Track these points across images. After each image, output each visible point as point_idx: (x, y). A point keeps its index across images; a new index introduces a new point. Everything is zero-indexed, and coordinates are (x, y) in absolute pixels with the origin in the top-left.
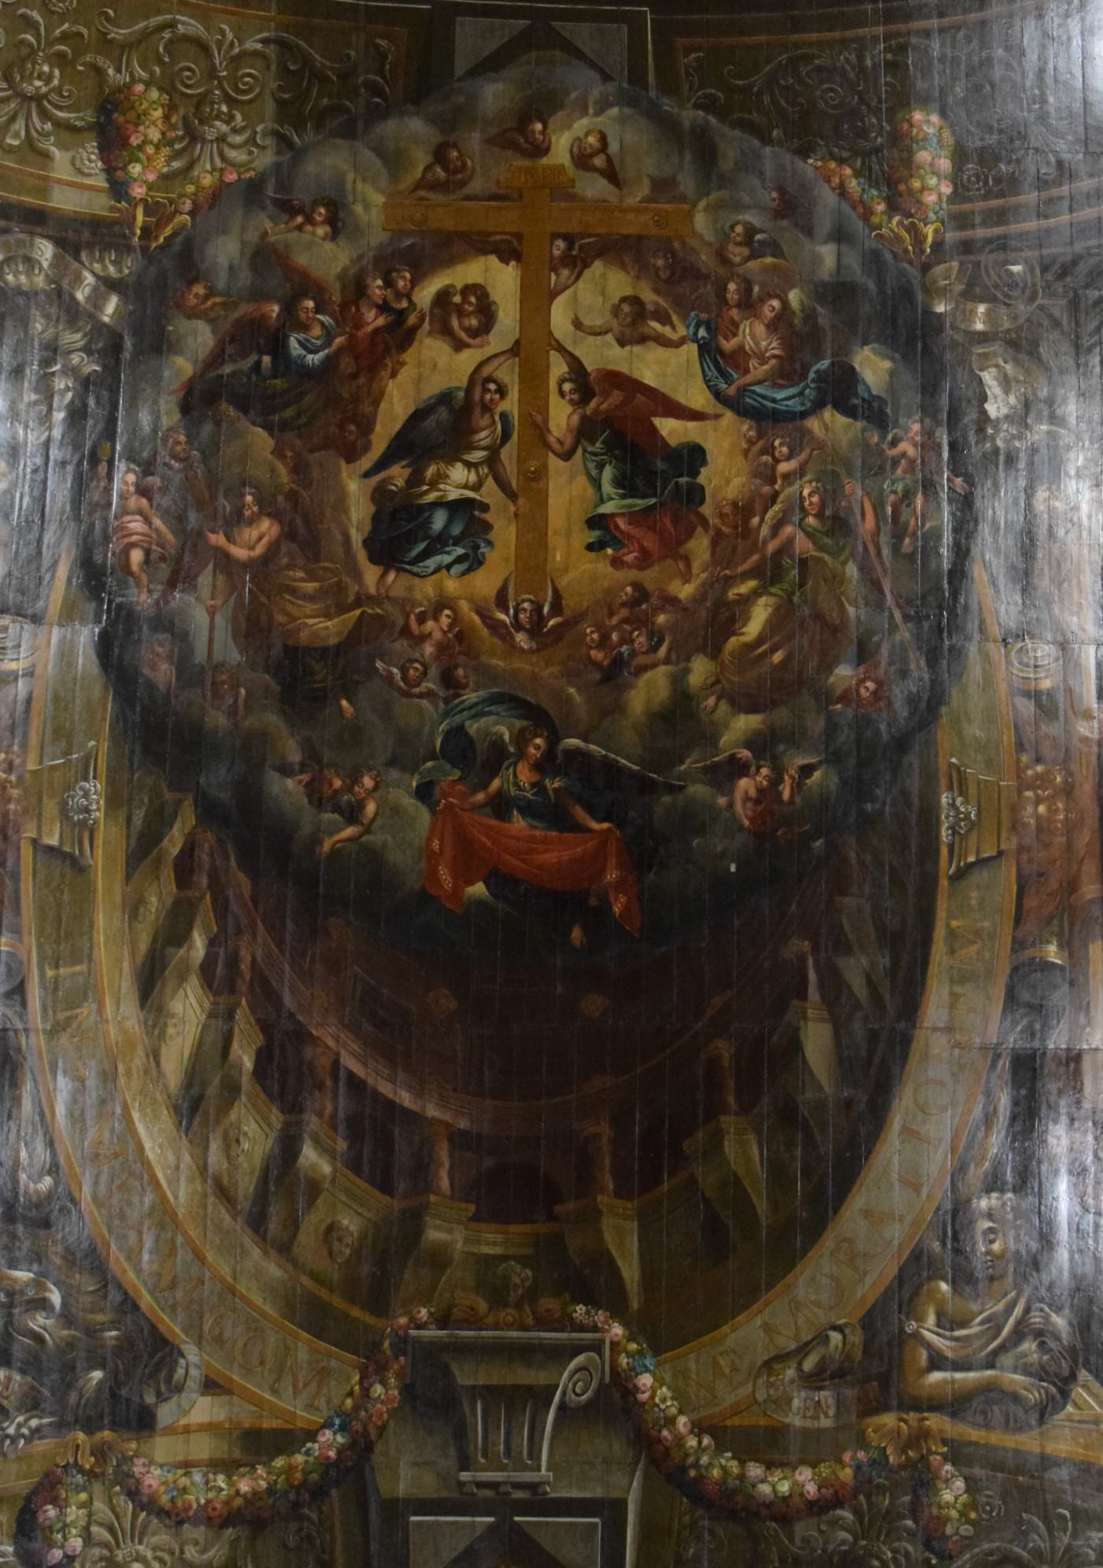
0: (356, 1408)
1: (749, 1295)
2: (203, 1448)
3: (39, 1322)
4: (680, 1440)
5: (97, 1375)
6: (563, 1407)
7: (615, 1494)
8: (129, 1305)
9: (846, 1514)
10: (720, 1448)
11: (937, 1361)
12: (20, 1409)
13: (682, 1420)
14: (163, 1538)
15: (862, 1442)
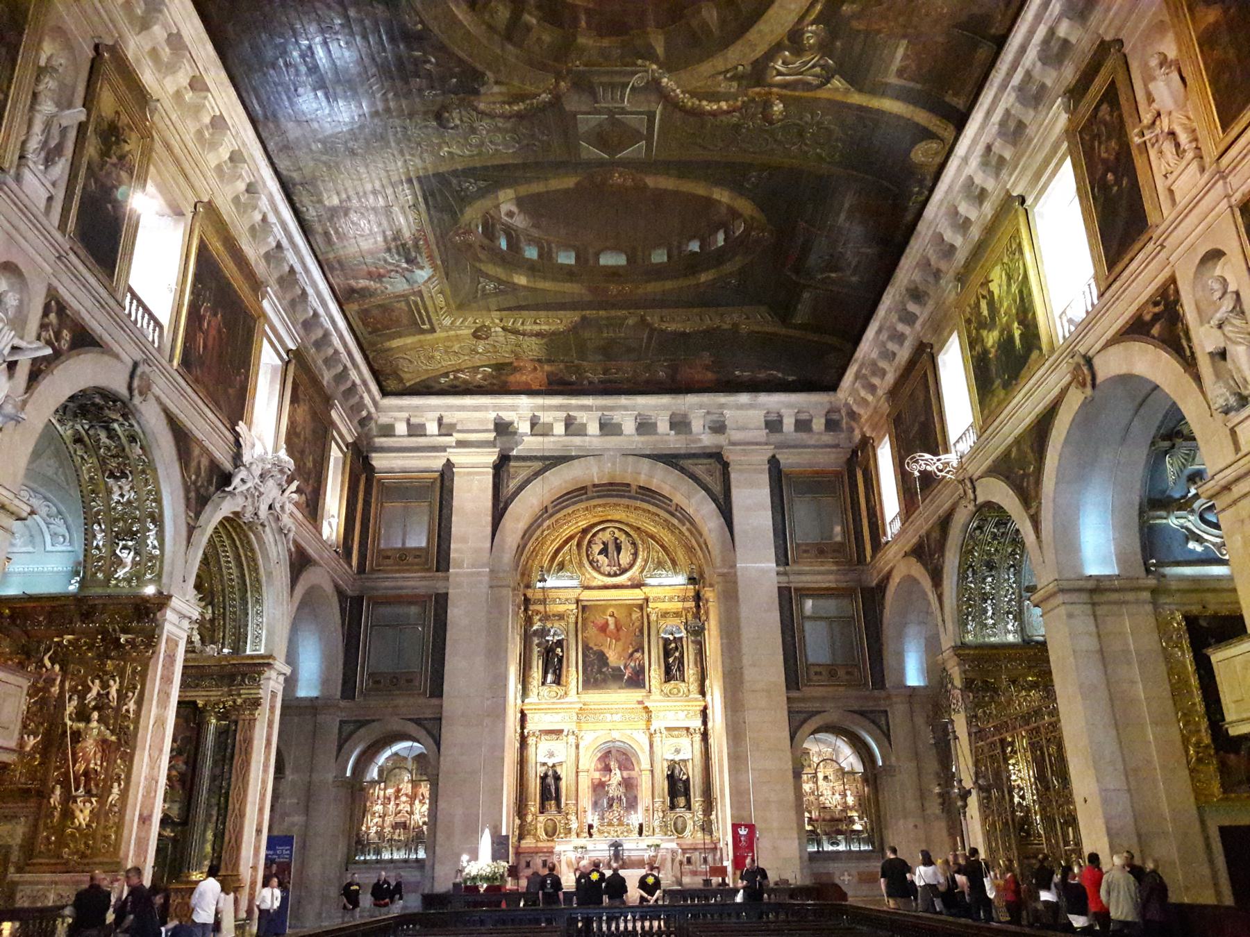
0: (555, 88)
1: (708, 55)
2: (500, 99)
3: (428, 66)
4: (677, 95)
5: (455, 80)
6: (633, 88)
7: (652, 109)
8: (460, 61)
9: (737, 114)
10: (692, 97)
11: (780, 73)
12: (428, 89)
13: (678, 91)
14: (488, 121)
15: (746, 95)
